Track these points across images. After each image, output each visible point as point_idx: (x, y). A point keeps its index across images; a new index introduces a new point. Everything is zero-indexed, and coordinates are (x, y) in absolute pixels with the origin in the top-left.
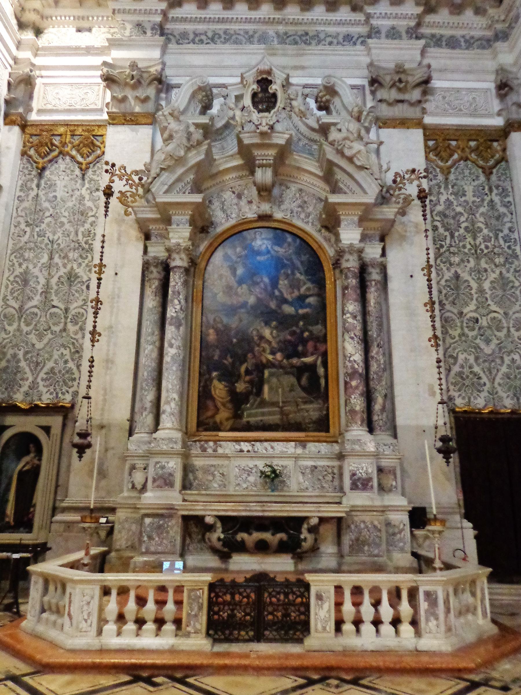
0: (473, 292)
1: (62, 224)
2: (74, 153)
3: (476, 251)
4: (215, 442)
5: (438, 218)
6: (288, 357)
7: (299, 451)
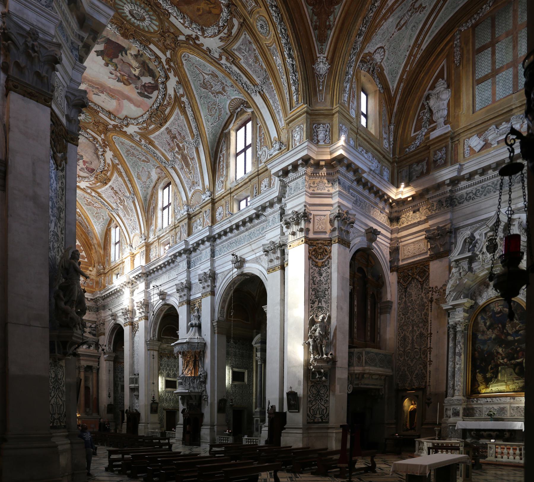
1: (416, 312)
2: (417, 277)
4: (477, 398)
6: (510, 360)
7: (512, 401)
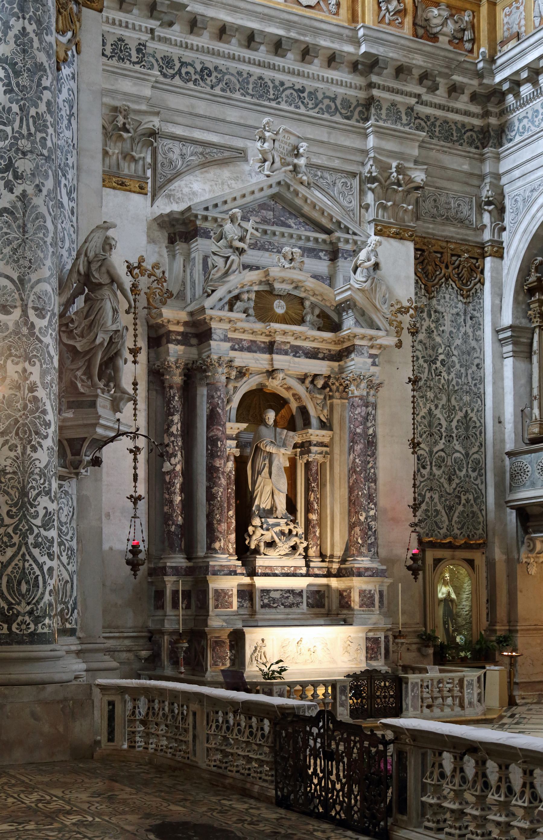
0: (443, 430)
3: (448, 387)
5: (419, 347)
